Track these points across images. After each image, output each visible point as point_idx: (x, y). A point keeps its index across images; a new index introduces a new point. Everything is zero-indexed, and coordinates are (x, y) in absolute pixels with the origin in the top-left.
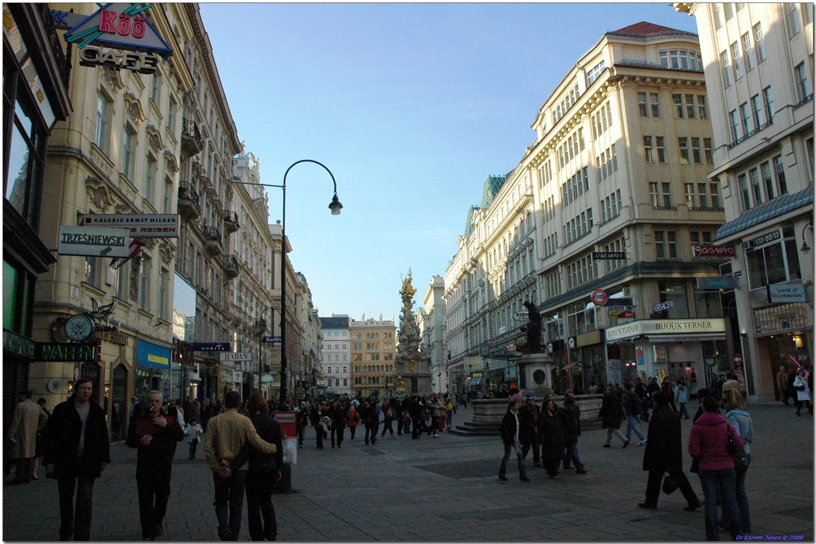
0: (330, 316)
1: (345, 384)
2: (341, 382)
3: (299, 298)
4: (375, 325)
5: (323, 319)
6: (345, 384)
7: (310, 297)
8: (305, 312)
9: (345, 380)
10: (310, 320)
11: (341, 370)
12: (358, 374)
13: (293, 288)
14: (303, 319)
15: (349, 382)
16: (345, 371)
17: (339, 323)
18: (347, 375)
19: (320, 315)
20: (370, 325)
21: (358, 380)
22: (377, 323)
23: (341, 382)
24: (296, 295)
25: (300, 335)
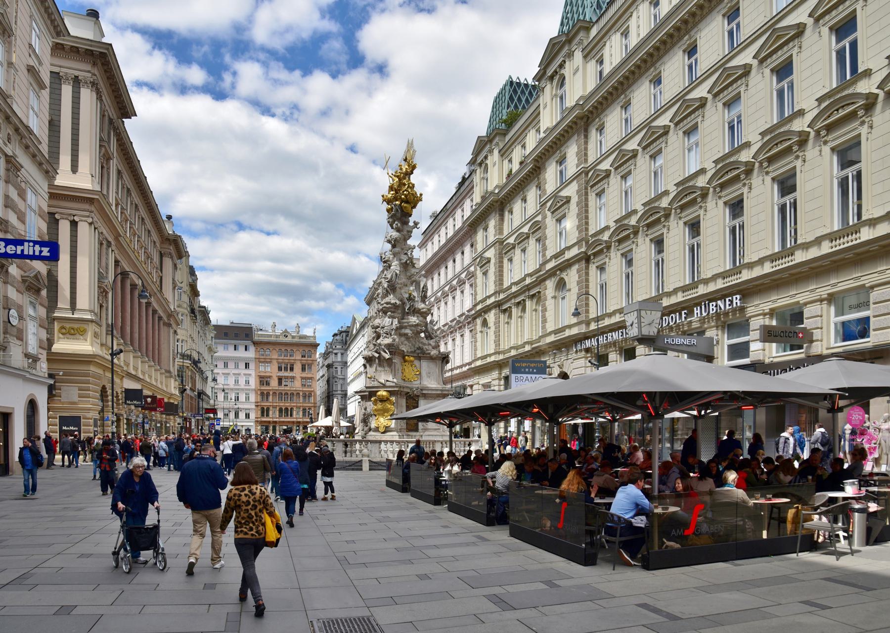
0: (228, 324)
1: (247, 416)
3: (168, 263)
4: (289, 339)
5: (218, 328)
6: (247, 416)
8: (185, 298)
10: (193, 311)
14: (174, 300)
15: (253, 416)
16: (247, 398)
21: (264, 411)
22: (293, 337)
23: (242, 415)
24: (161, 256)
25: (169, 325)
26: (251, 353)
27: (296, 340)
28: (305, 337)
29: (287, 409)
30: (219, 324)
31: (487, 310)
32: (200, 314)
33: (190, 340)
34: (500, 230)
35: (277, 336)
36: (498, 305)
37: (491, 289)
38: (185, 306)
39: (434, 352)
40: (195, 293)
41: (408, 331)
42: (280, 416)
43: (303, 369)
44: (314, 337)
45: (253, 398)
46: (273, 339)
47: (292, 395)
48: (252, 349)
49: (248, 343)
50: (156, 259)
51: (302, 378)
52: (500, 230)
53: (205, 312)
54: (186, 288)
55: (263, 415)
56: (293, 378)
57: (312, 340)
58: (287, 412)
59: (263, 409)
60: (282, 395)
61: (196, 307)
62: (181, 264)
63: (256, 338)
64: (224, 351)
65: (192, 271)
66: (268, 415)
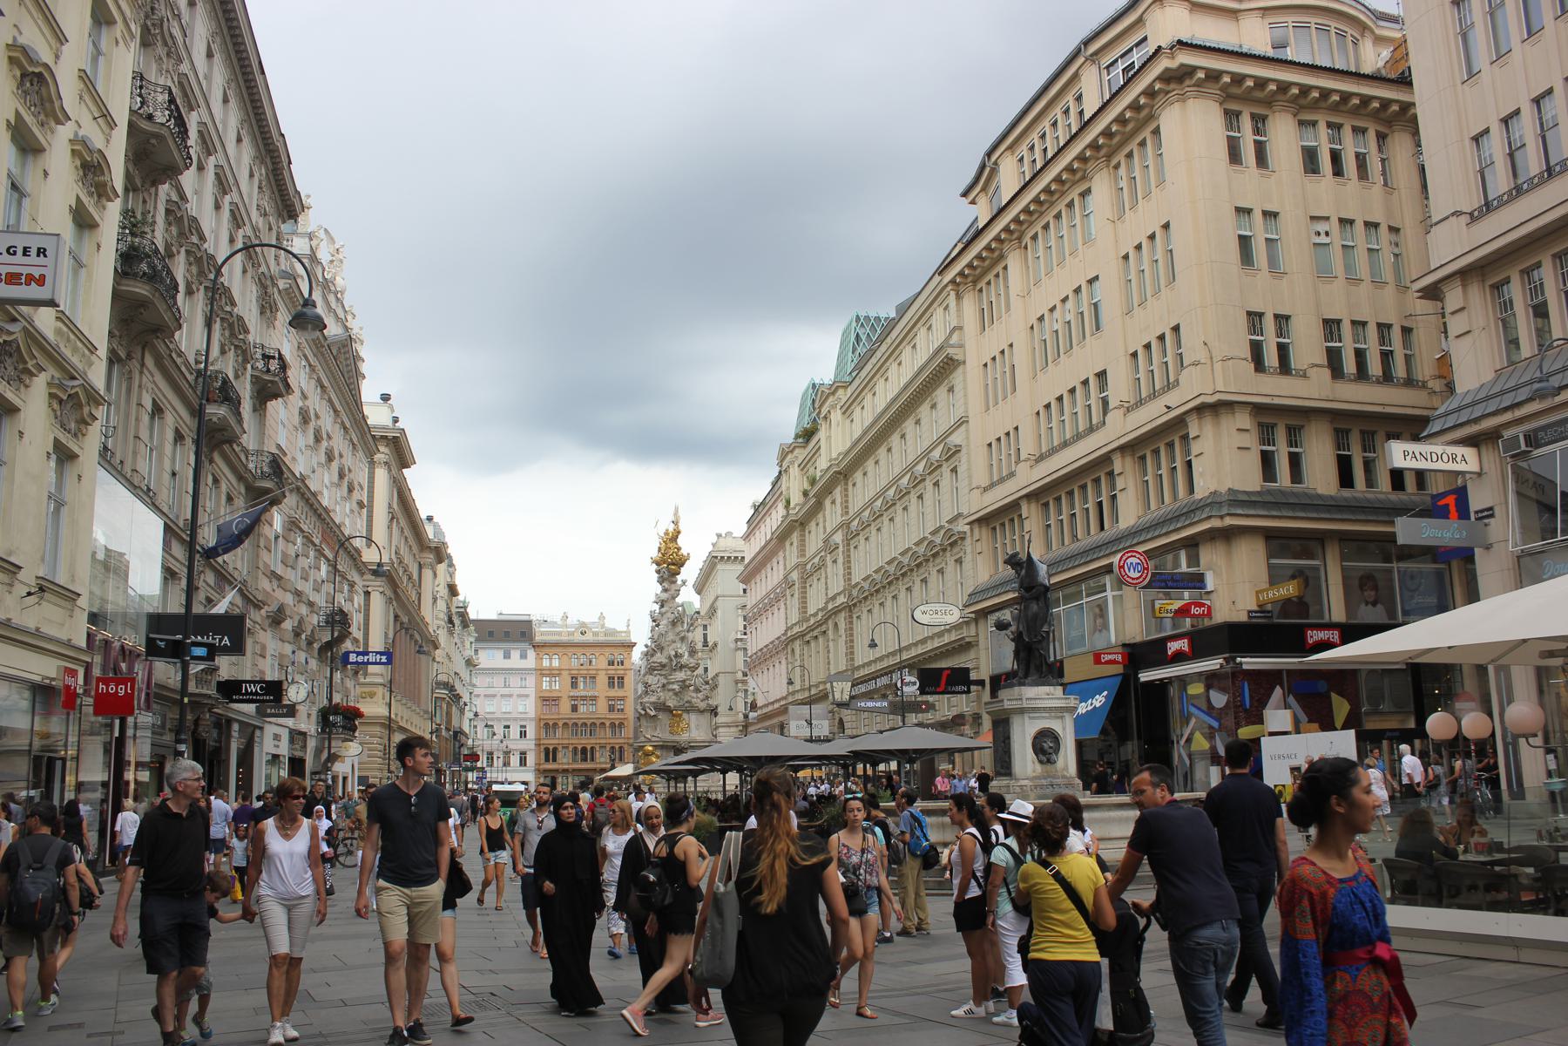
0: (494, 617)
1: (523, 762)
2: (515, 760)
3: (427, 573)
4: (589, 638)
5: (480, 623)
6: (523, 762)
7: (452, 575)
8: (441, 605)
9: (523, 754)
10: (451, 621)
11: (515, 732)
12: (551, 742)
13: (415, 549)
16: (523, 734)
17: (514, 632)
18: (529, 744)
19: (473, 615)
20: (578, 638)
21: (550, 754)
22: (596, 634)
23: (515, 760)
26: (531, 661)
27: (601, 638)
28: (614, 632)
29: (584, 750)
30: (482, 617)
31: (793, 639)
32: (458, 618)
33: (446, 661)
34: (802, 552)
35: (571, 634)
36: (802, 635)
37: (794, 618)
38: (442, 616)
39: (702, 705)
40: (453, 590)
41: (675, 687)
42: (574, 760)
43: (611, 684)
44: (628, 632)
45: (531, 733)
46: (564, 638)
47: (592, 727)
48: (531, 654)
49: (525, 645)
50: (415, 576)
51: (609, 699)
52: (802, 552)
53: (463, 615)
54: (443, 591)
55: (547, 760)
56: (594, 698)
57: (621, 638)
58: (585, 753)
59: (547, 750)
60: (575, 727)
61: (454, 610)
62: (441, 568)
63: (538, 638)
64: (490, 657)
65: (451, 565)
66: (554, 760)
